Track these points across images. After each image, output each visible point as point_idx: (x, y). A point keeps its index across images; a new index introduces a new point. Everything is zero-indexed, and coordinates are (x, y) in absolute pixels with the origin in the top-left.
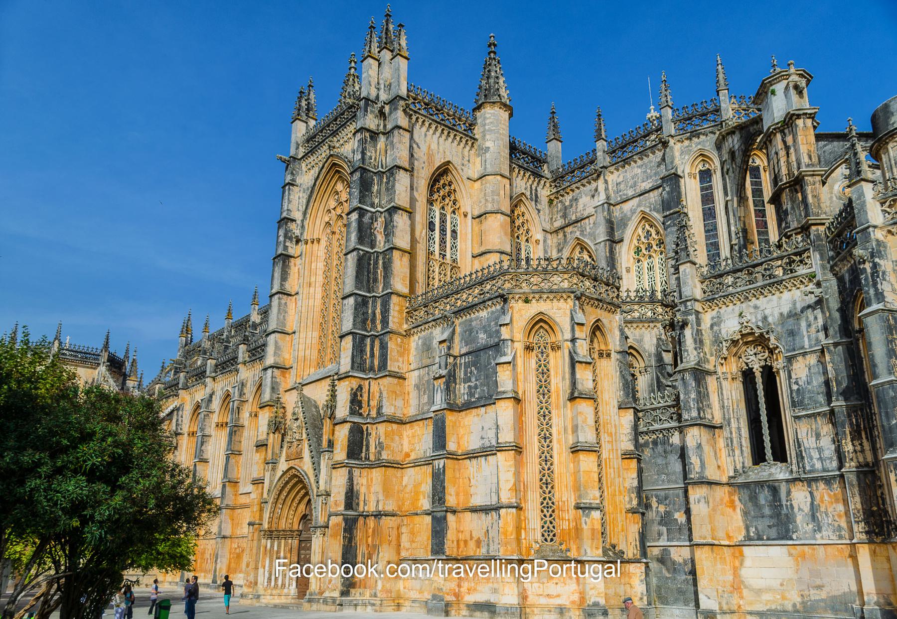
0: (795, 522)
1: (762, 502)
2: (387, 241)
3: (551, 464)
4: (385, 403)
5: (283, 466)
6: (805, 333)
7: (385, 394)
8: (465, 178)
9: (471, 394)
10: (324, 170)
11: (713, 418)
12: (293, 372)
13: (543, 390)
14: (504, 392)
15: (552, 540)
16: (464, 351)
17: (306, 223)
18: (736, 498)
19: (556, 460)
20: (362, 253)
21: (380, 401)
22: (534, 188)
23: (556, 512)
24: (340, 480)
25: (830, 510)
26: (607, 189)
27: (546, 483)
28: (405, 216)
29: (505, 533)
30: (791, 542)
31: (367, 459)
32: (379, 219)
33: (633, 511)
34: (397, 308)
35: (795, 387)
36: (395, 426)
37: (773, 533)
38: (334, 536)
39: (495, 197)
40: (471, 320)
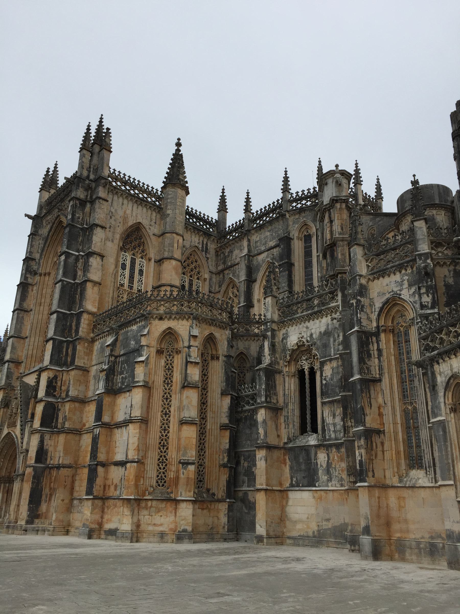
0: (318, 474)
1: (301, 460)
2: (84, 275)
3: (168, 432)
4: (71, 388)
6: (332, 346)
7: (71, 382)
8: (151, 234)
9: (123, 383)
10: (55, 225)
11: (278, 402)
12: (23, 365)
13: (168, 380)
14: (138, 382)
15: (163, 485)
16: (122, 353)
17: (41, 261)
18: (287, 458)
19: (171, 430)
20: (65, 283)
21: (69, 387)
22: (205, 243)
23: (168, 465)
24: (35, 441)
25: (337, 466)
26: (249, 245)
27: (163, 445)
28: (99, 259)
29: (128, 481)
30: (314, 489)
31: (56, 427)
32: (81, 260)
33: (224, 466)
34: (87, 322)
35: (324, 382)
36: (77, 405)
37: (306, 482)
38: (27, 481)
39: (171, 248)
40: (128, 332)
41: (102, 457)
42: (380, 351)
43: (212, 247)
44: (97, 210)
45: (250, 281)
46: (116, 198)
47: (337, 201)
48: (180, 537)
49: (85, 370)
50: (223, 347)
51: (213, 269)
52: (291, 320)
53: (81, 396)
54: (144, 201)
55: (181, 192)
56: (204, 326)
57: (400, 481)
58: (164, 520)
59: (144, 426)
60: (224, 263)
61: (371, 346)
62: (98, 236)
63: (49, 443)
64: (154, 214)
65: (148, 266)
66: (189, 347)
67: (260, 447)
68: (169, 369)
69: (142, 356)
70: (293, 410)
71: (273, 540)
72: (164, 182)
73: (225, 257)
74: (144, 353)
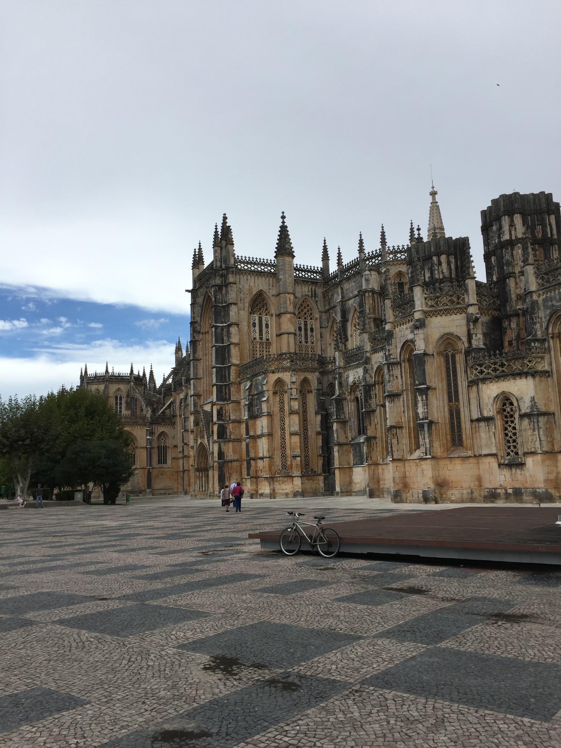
4: (231, 415)
5: (199, 441)
9: (258, 412)
12: (202, 397)
13: (282, 409)
14: (264, 413)
19: (286, 438)
22: (313, 290)
26: (342, 292)
27: (283, 447)
29: (265, 468)
31: (227, 438)
33: (320, 456)
34: (234, 372)
36: (236, 424)
37: (359, 462)
38: (216, 470)
41: (252, 455)
42: (375, 394)
43: (320, 291)
44: (230, 292)
45: (345, 320)
46: (242, 276)
47: (366, 292)
48: (295, 495)
49: (238, 402)
50: (314, 384)
51: (322, 309)
52: (349, 367)
53: (238, 419)
54: (262, 272)
55: (287, 259)
56: (300, 373)
57: (383, 461)
58: (287, 487)
59: (270, 438)
60: (329, 304)
61: (372, 392)
62: (233, 310)
63: (223, 447)
64: (271, 279)
65: (271, 320)
66: (291, 389)
67: (335, 445)
68: (282, 403)
69: (264, 397)
70: (353, 422)
71: (345, 494)
72: (275, 252)
73: (330, 299)
74: (266, 395)
